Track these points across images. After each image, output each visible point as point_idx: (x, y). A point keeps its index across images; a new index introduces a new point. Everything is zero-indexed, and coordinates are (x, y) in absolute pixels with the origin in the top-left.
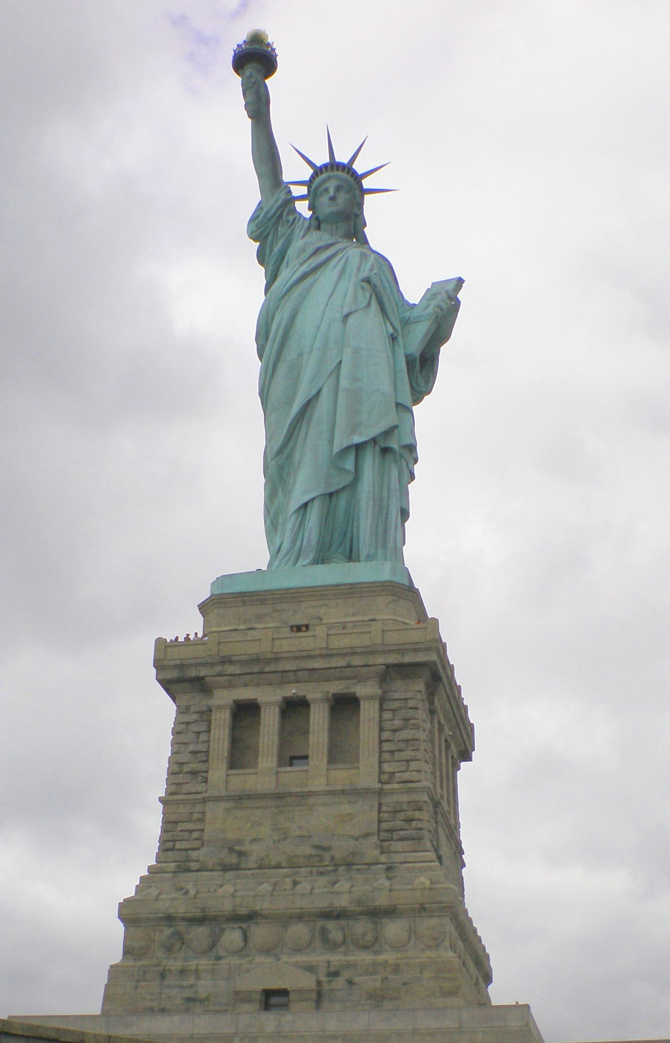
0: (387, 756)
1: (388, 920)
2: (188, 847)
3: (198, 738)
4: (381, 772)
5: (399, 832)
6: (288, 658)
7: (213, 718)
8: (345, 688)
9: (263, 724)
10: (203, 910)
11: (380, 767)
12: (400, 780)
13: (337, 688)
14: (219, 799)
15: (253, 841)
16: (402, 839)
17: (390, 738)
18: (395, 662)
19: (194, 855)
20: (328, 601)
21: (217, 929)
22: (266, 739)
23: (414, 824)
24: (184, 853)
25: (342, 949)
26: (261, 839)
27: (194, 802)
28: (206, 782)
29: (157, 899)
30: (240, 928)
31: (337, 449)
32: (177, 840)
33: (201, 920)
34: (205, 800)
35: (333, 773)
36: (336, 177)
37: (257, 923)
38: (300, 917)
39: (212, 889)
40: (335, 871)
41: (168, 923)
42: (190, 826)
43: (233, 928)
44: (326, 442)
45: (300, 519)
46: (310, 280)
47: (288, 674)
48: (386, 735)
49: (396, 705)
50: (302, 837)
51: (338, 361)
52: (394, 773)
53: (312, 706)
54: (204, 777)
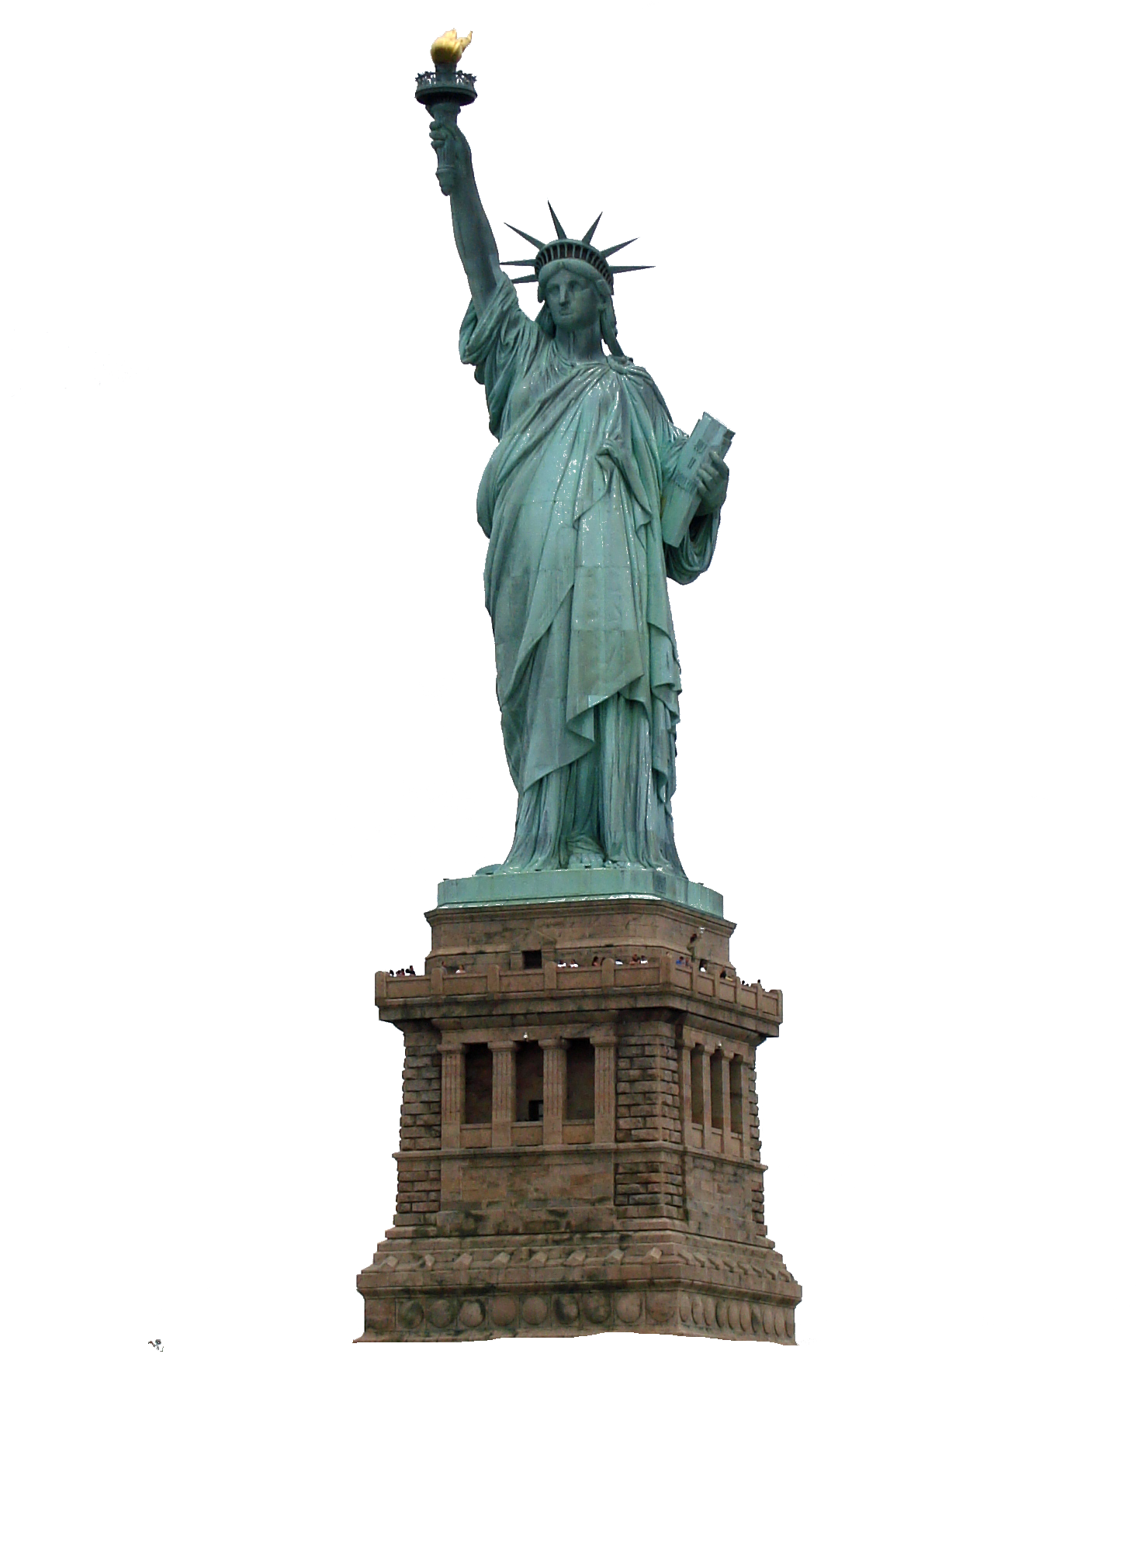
0: (623, 1110)
1: (620, 1294)
2: (425, 1209)
3: (430, 1085)
4: (618, 1128)
5: (634, 1196)
6: (517, 1000)
7: (443, 1064)
8: (579, 1032)
9: (495, 1072)
10: (440, 1283)
11: (617, 1124)
12: (636, 1139)
13: (569, 1032)
14: (452, 1158)
15: (489, 1204)
16: (637, 1204)
17: (627, 1091)
18: (628, 1007)
19: (432, 1217)
20: (562, 919)
21: (455, 1303)
22: (499, 1090)
23: (650, 1186)
24: (422, 1216)
25: (576, 1324)
26: (497, 1203)
27: (428, 1160)
28: (440, 1137)
29: (394, 1272)
30: (478, 1301)
31: (570, 716)
32: (415, 1202)
33: (440, 1292)
34: (439, 1159)
35: (568, 1129)
36: (565, 268)
37: (494, 1296)
38: (537, 1290)
39: (450, 1259)
40: (570, 1239)
41: (407, 1296)
42: (426, 1186)
43: (471, 1302)
44: (559, 700)
45: (535, 797)
46: (534, 458)
47: (519, 1017)
48: (623, 1087)
49: (634, 1051)
50: (538, 1200)
51: (570, 586)
52: (630, 1130)
53: (545, 1052)
54: (437, 1131)
